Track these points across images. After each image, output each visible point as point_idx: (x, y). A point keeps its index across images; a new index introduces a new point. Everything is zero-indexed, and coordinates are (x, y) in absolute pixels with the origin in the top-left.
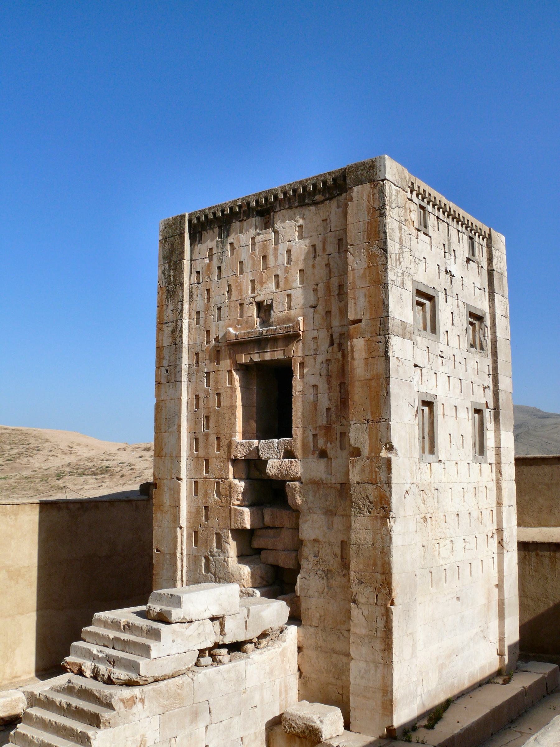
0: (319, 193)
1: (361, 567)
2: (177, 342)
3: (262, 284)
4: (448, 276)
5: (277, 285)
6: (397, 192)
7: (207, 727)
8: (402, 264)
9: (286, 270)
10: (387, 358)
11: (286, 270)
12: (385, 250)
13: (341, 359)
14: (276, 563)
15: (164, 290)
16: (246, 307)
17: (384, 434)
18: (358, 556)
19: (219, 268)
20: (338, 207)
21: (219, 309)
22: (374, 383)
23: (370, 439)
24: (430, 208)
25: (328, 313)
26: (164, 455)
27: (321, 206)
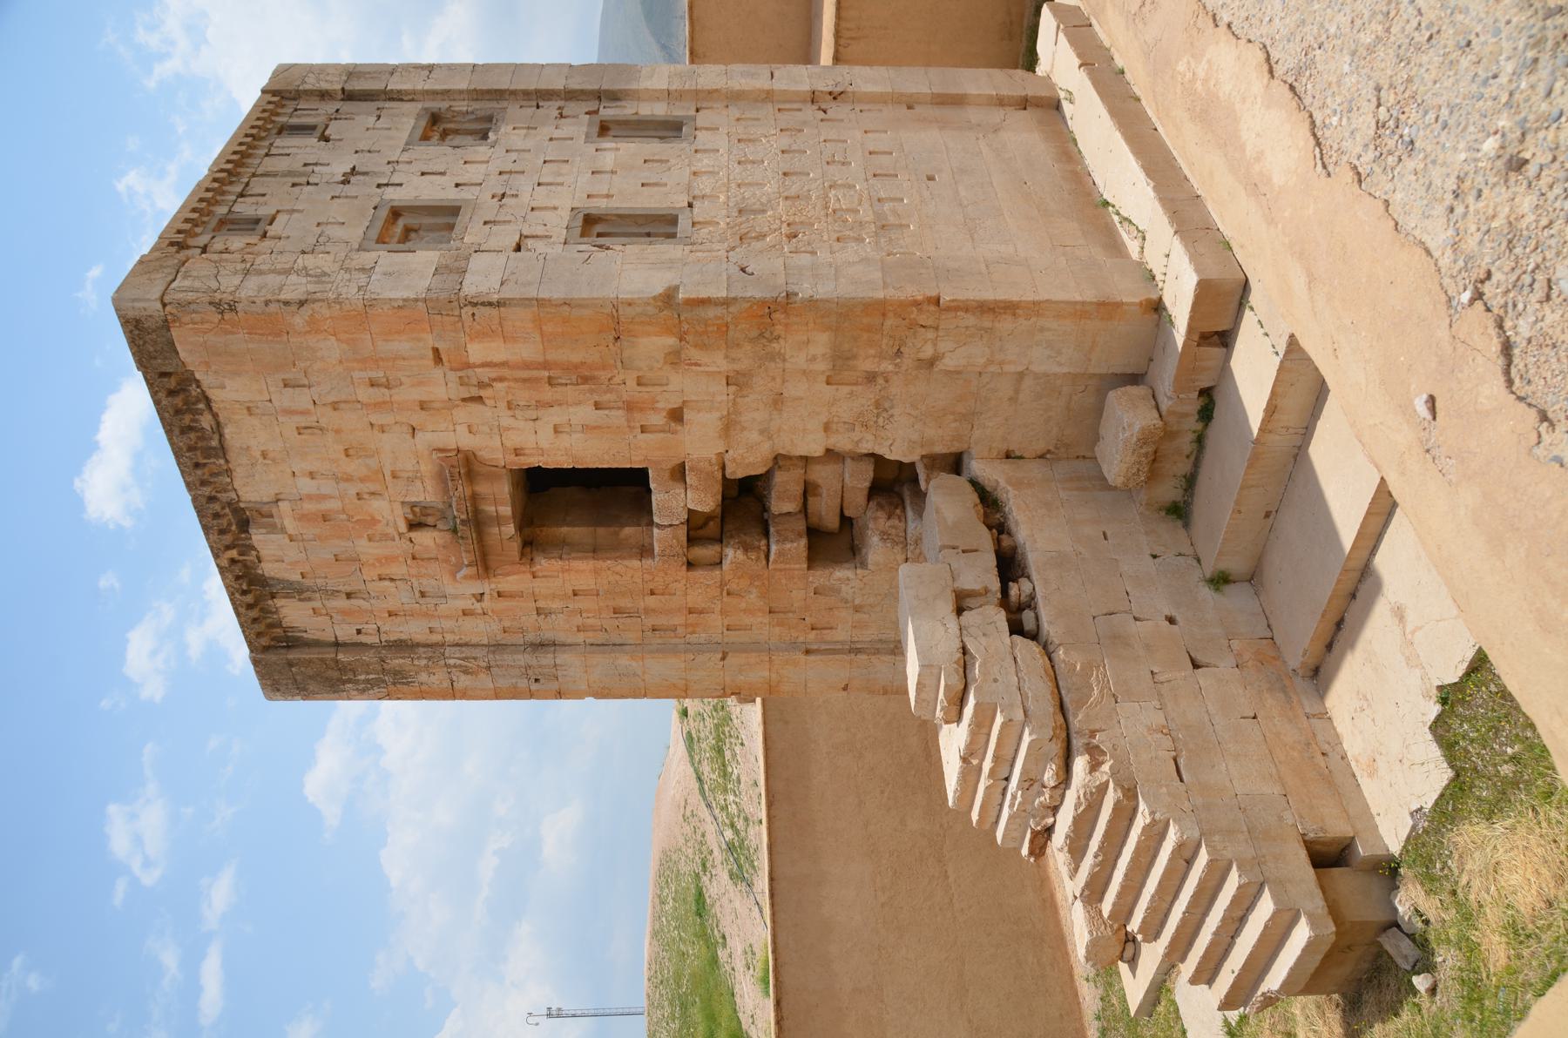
0: (196, 421)
1: (872, 352)
3: (374, 521)
4: (353, 179)
6: (185, 277)
7: (1136, 619)
8: (326, 270)
10: (499, 304)
12: (302, 303)
13: (505, 384)
14: (866, 492)
15: (391, 688)
17: (639, 310)
18: (855, 357)
19: (349, 596)
20: (223, 387)
22: (548, 328)
23: (649, 335)
24: (222, 210)
25: (423, 406)
27: (221, 419)
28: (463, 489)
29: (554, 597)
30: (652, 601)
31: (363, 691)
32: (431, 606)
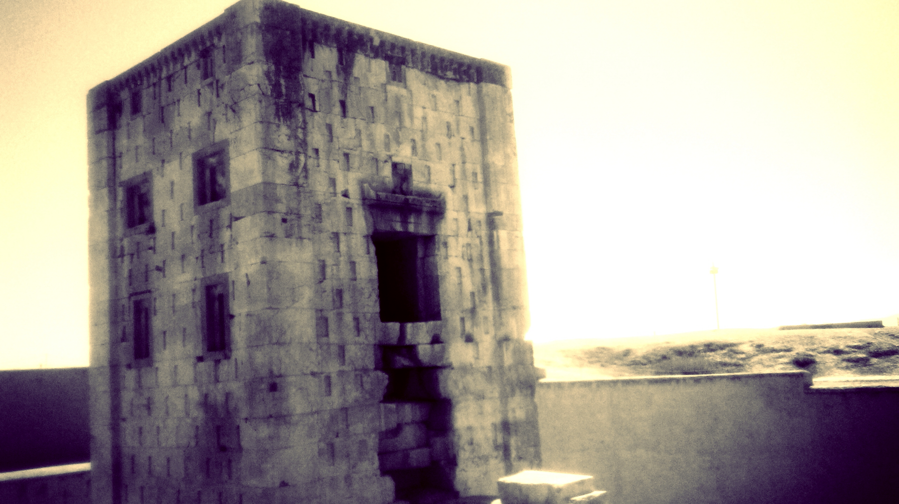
0: (450, 70)
1: (520, 444)
2: (301, 181)
3: (399, 143)
5: (414, 148)
9: (423, 139)
11: (423, 139)
16: (381, 164)
19: (343, 104)
21: (346, 155)
25: (466, 198)
26: (288, 341)
28: (427, 206)
29: (349, 247)
30: (348, 318)
31: (267, 74)
32: (337, 157)
